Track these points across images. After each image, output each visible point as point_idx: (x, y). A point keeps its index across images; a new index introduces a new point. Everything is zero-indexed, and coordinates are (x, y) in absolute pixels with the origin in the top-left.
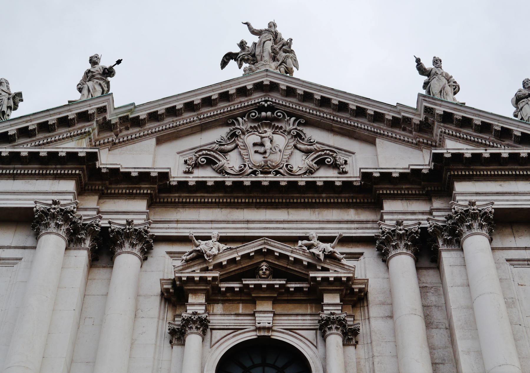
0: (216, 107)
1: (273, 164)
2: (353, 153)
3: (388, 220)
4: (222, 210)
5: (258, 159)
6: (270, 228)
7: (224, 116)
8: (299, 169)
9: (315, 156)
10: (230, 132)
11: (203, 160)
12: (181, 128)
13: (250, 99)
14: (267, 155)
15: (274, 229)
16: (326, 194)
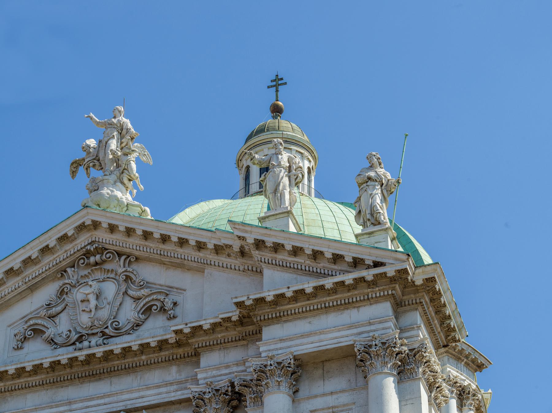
0: (41, 265)
1: (101, 323)
2: (185, 290)
3: (201, 379)
4: (48, 391)
5: (85, 319)
6: (92, 406)
7: (52, 272)
8: (128, 321)
9: (144, 302)
10: (59, 289)
11: (29, 333)
12: (8, 298)
13: (76, 245)
14: (93, 313)
15: (95, 406)
16: (146, 355)
